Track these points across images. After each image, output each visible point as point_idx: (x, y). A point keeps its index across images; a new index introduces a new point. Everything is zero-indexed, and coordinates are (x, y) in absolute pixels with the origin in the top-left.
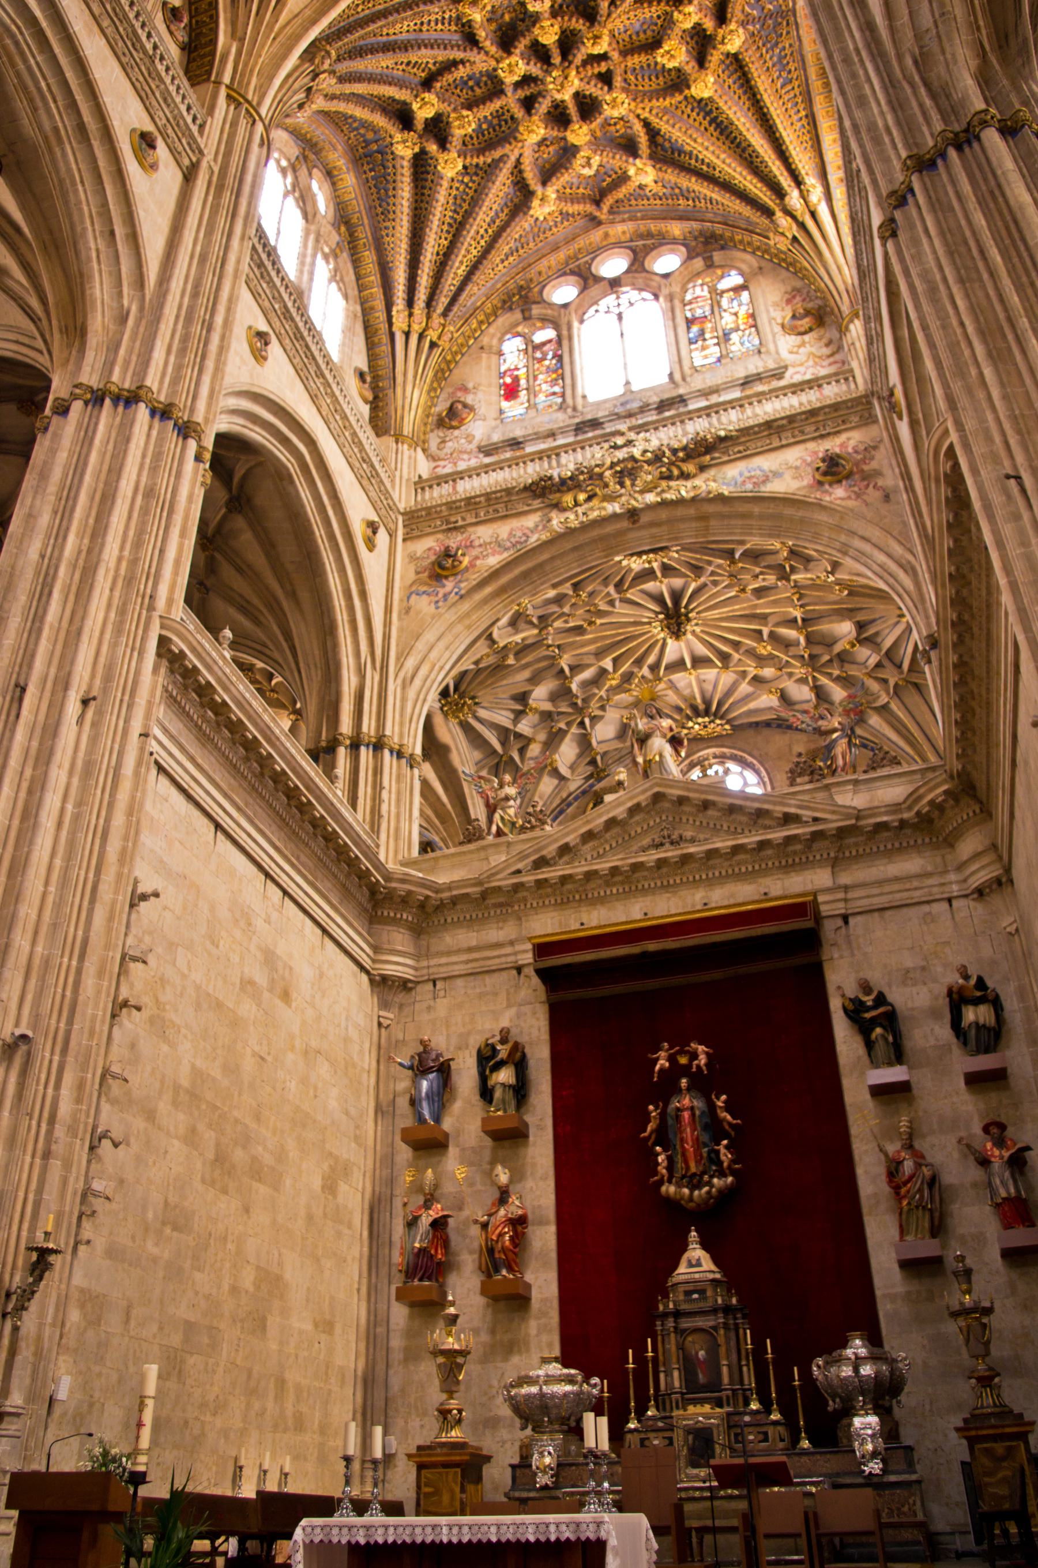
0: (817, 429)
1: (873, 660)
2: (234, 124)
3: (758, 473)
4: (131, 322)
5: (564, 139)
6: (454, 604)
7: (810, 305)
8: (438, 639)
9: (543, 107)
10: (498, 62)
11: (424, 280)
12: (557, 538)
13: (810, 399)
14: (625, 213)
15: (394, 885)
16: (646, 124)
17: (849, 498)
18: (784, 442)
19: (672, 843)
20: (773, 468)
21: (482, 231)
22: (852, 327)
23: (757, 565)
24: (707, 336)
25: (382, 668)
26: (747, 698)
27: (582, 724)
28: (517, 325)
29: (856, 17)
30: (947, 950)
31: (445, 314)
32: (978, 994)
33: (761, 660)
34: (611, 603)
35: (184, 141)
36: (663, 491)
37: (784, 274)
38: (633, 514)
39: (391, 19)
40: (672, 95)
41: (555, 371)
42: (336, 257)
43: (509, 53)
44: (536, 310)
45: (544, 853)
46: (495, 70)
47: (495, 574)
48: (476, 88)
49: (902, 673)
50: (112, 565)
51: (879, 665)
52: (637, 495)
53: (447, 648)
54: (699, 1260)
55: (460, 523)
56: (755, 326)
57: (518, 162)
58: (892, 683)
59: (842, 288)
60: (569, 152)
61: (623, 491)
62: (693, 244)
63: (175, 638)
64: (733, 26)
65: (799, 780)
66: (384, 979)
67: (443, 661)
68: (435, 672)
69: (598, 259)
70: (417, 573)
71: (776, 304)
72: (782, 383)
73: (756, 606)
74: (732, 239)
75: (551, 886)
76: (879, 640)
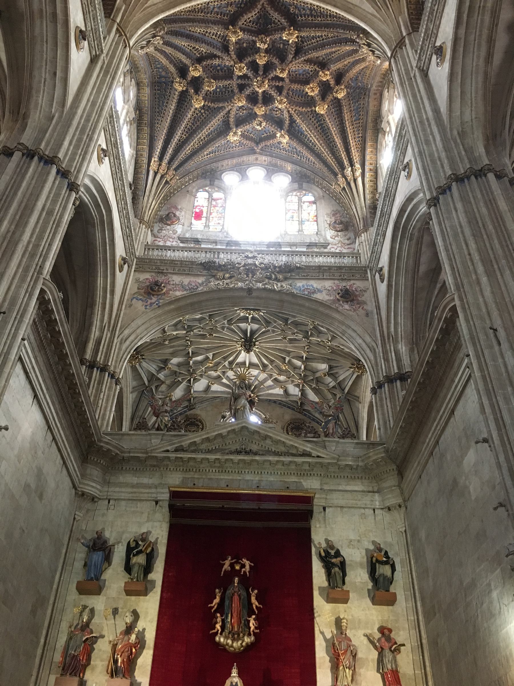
0: (340, 276)
1: (332, 384)
2: (118, 44)
3: (311, 287)
4: (54, 122)
5: (252, 109)
6: (154, 309)
7: (343, 220)
8: (143, 324)
9: (248, 91)
10: (235, 63)
11: (170, 151)
12: (212, 291)
13: (331, 261)
14: (268, 152)
15: (102, 444)
16: (291, 116)
17: (351, 310)
18: (325, 277)
19: (246, 452)
20: (318, 288)
21: (202, 138)
22: (363, 235)
23: (296, 328)
25: (112, 331)
26: (270, 387)
27: (190, 380)
28: (206, 186)
30: (371, 534)
31: (176, 169)
32: (385, 559)
33: (281, 372)
34: (223, 328)
35: (96, 42)
36: (266, 284)
37: (334, 202)
38: (250, 291)
39: (195, 24)
40: (306, 108)
42: (131, 124)
43: (241, 62)
44: (216, 182)
45: (183, 444)
46: (231, 66)
47: (178, 300)
48: (220, 71)
49: (344, 393)
50: (25, 243)
51: (334, 387)
52: (253, 282)
53: (146, 329)
54: (237, 683)
55: (165, 271)
56: (317, 221)
57: (229, 112)
58: (338, 396)
59: (360, 217)
60: (255, 116)
61: (247, 278)
62: (296, 176)
63: (48, 292)
64: (343, 87)
65: (309, 435)
66: (83, 494)
67: (142, 335)
68: (137, 340)
69: (250, 168)
70: (138, 289)
71: (327, 214)
72: (326, 250)
73: (286, 347)
74: (314, 179)
75: (182, 461)
76: (337, 376)
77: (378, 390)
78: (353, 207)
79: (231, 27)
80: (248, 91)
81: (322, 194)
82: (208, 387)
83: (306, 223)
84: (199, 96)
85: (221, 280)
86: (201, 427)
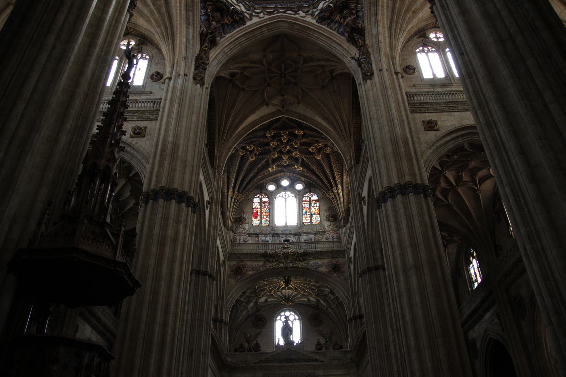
0: (332, 256)
1: (332, 297)
7: (333, 213)
17: (337, 277)
18: (324, 257)
24: (308, 214)
27: (257, 299)
29: (362, 221)
36: (294, 264)
38: (286, 268)
41: (268, 213)
44: (264, 191)
57: (268, 159)
58: (336, 303)
70: (231, 271)
71: (325, 210)
74: (317, 187)
77: (363, 276)
78: (338, 209)
79: (268, 131)
80: (278, 150)
81: (322, 196)
82: (266, 301)
83: (314, 216)
84: (252, 155)
85: (271, 263)
86: (264, 321)
